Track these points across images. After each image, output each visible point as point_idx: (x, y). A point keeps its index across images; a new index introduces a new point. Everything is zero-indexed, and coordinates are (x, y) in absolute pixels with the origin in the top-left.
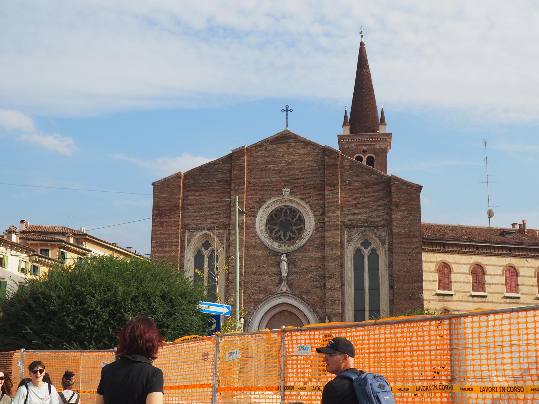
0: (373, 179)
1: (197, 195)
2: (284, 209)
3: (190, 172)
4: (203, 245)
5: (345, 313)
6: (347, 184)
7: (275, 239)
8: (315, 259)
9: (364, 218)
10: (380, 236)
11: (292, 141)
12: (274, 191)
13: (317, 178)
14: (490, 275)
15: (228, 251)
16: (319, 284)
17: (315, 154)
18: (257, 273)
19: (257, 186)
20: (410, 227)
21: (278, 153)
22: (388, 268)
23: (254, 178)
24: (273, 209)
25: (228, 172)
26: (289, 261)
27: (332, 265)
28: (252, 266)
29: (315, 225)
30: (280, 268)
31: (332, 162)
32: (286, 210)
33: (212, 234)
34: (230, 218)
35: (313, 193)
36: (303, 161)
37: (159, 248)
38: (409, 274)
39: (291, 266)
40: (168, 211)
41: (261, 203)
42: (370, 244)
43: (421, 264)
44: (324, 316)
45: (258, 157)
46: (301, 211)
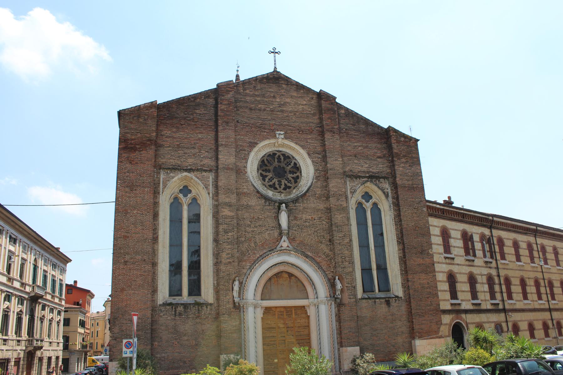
0: (370, 130)
1: (174, 130)
2: (276, 154)
3: (165, 104)
4: (181, 191)
5: (355, 273)
6: (344, 132)
7: (269, 187)
8: (318, 210)
9: (364, 168)
10: (383, 189)
11: (283, 82)
12: (267, 133)
13: (312, 123)
14: (454, 238)
15: (215, 198)
16: (324, 239)
17: (309, 98)
18: (251, 226)
19: (247, 126)
20: (413, 179)
21: (268, 93)
22: (394, 222)
23: (243, 117)
24: (264, 153)
25: (212, 107)
26: (290, 212)
27: (338, 218)
28: (245, 217)
29: (315, 173)
30: (279, 220)
31: (329, 106)
32: (279, 156)
33: (194, 177)
34: (217, 159)
35: (309, 139)
36: (296, 103)
37: (127, 189)
38: (417, 229)
39: (291, 218)
40: (138, 145)
41: (253, 145)
42: (371, 197)
43: (427, 218)
44: (332, 276)
45: (247, 95)
46: (296, 158)
